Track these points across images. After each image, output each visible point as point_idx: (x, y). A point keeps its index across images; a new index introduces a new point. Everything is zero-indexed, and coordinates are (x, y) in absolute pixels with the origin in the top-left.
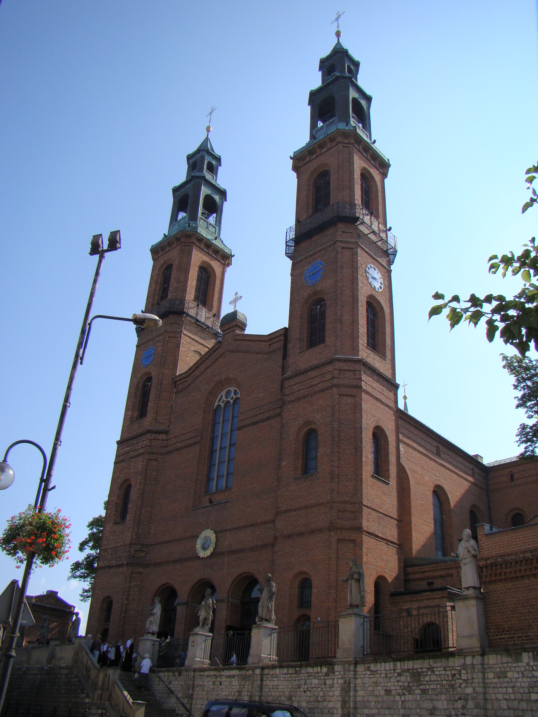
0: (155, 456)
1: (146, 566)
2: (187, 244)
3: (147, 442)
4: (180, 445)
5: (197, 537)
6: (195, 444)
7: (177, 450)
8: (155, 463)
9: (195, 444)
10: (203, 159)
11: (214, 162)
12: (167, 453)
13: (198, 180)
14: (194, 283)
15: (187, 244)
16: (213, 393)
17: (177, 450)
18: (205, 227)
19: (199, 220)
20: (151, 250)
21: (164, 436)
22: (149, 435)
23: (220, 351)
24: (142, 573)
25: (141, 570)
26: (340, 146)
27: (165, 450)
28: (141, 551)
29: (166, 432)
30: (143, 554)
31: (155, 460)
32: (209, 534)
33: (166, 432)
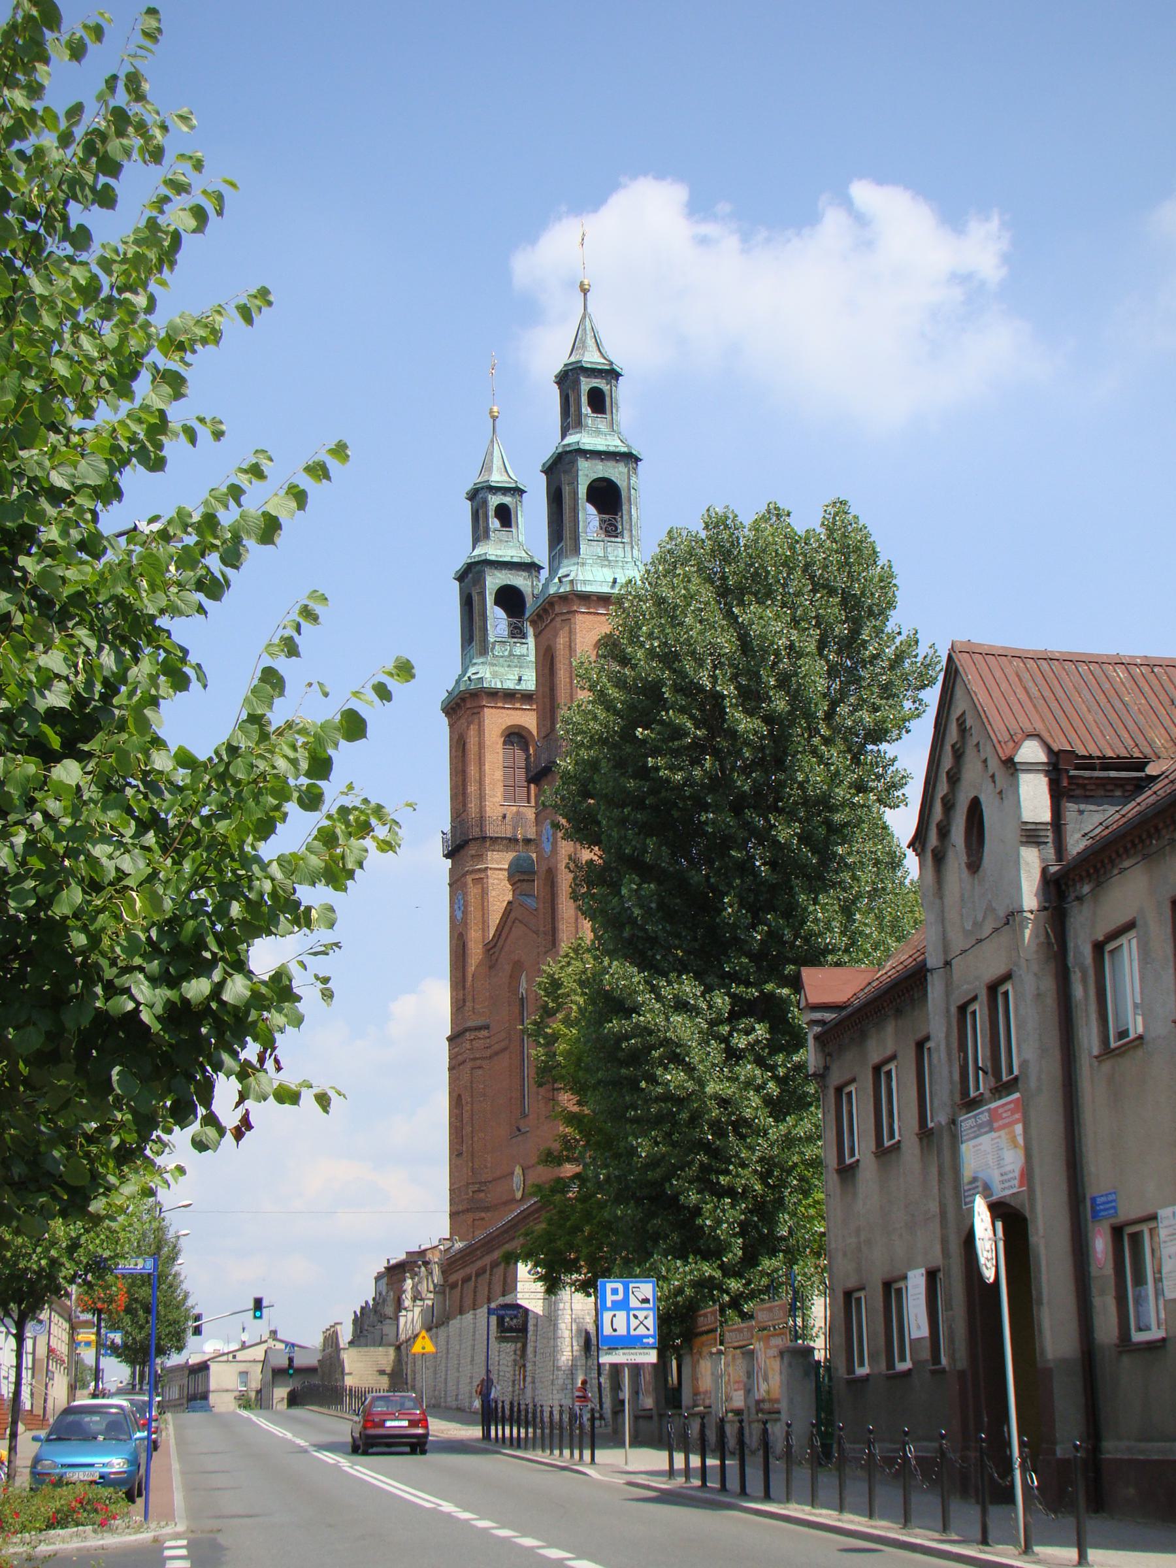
0: (478, 1062)
1: (487, 1209)
2: (475, 711)
3: (468, 1046)
4: (497, 1047)
5: (513, 1173)
6: (505, 1049)
7: (497, 1054)
8: (480, 1072)
9: (505, 1049)
10: (485, 502)
11: (507, 500)
12: (490, 1057)
13: (478, 568)
14: (499, 774)
15: (475, 711)
16: (514, 977)
17: (497, 1054)
18: (506, 653)
19: (493, 648)
20: (443, 710)
21: (485, 1033)
22: (467, 1034)
23: (513, 915)
24: (483, 1219)
25: (483, 1215)
26: (559, 619)
27: (488, 1053)
28: (479, 1191)
29: (486, 1027)
30: (482, 1195)
31: (480, 1068)
32: (518, 1170)
33: (486, 1027)
